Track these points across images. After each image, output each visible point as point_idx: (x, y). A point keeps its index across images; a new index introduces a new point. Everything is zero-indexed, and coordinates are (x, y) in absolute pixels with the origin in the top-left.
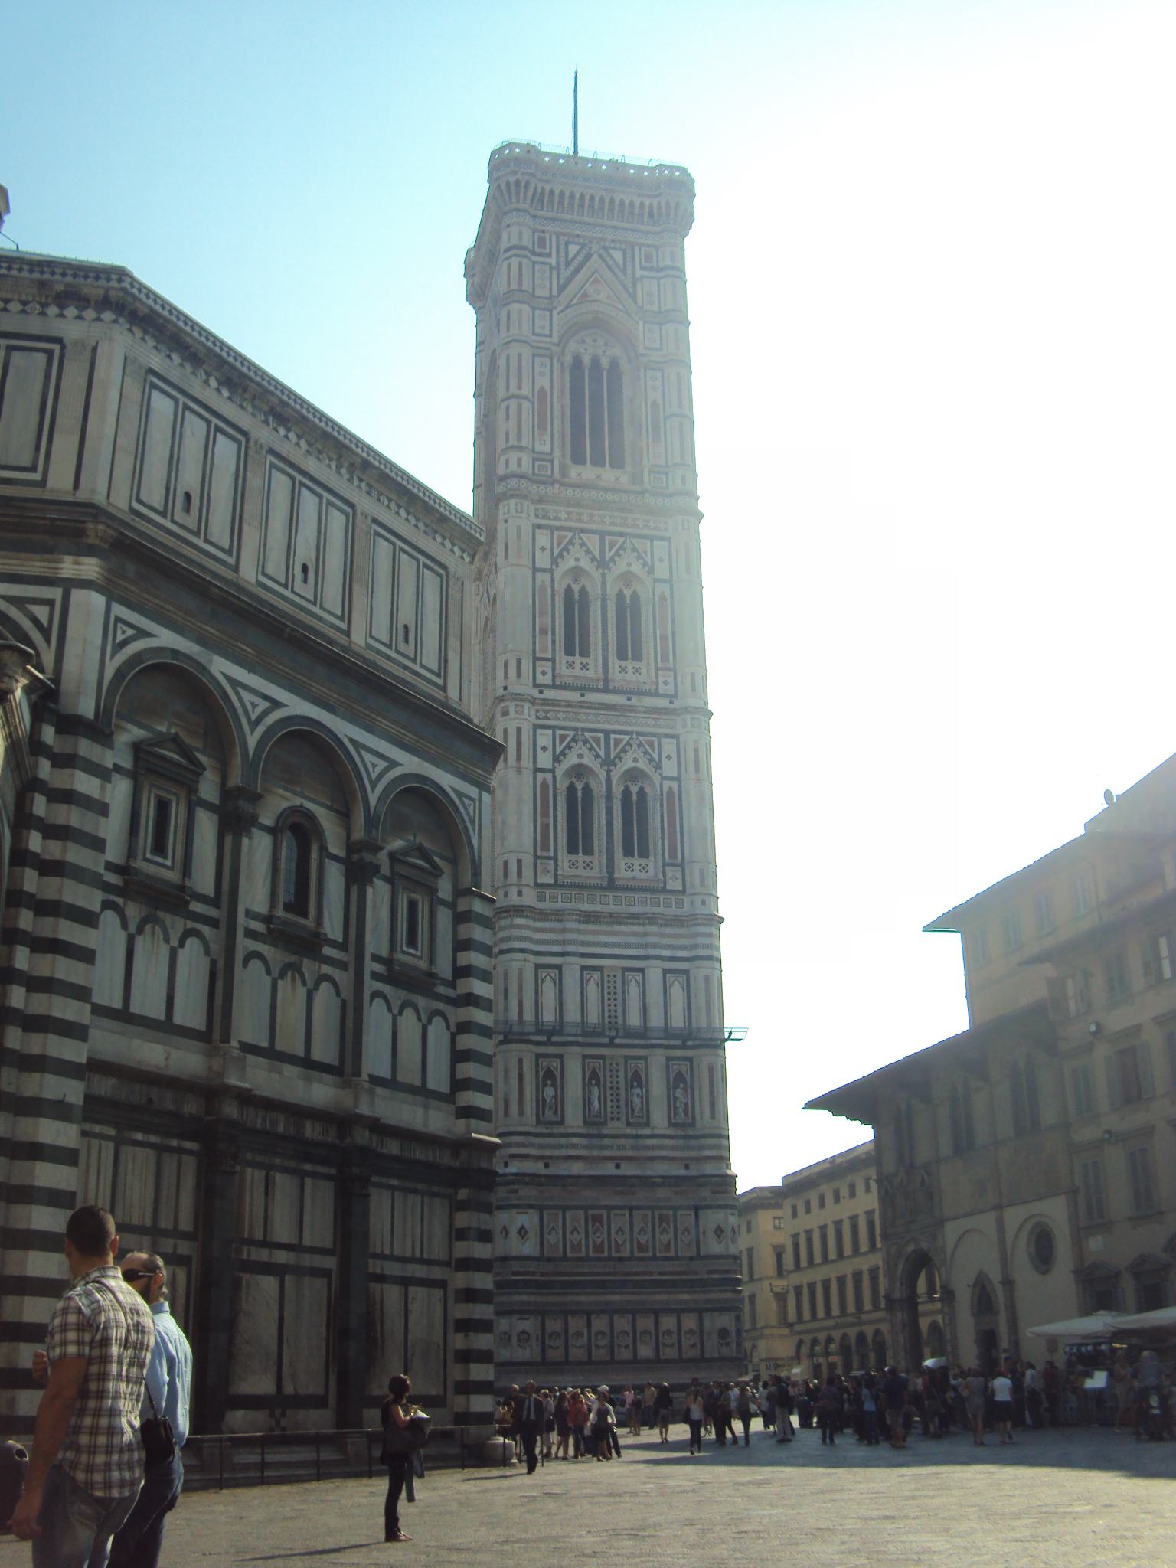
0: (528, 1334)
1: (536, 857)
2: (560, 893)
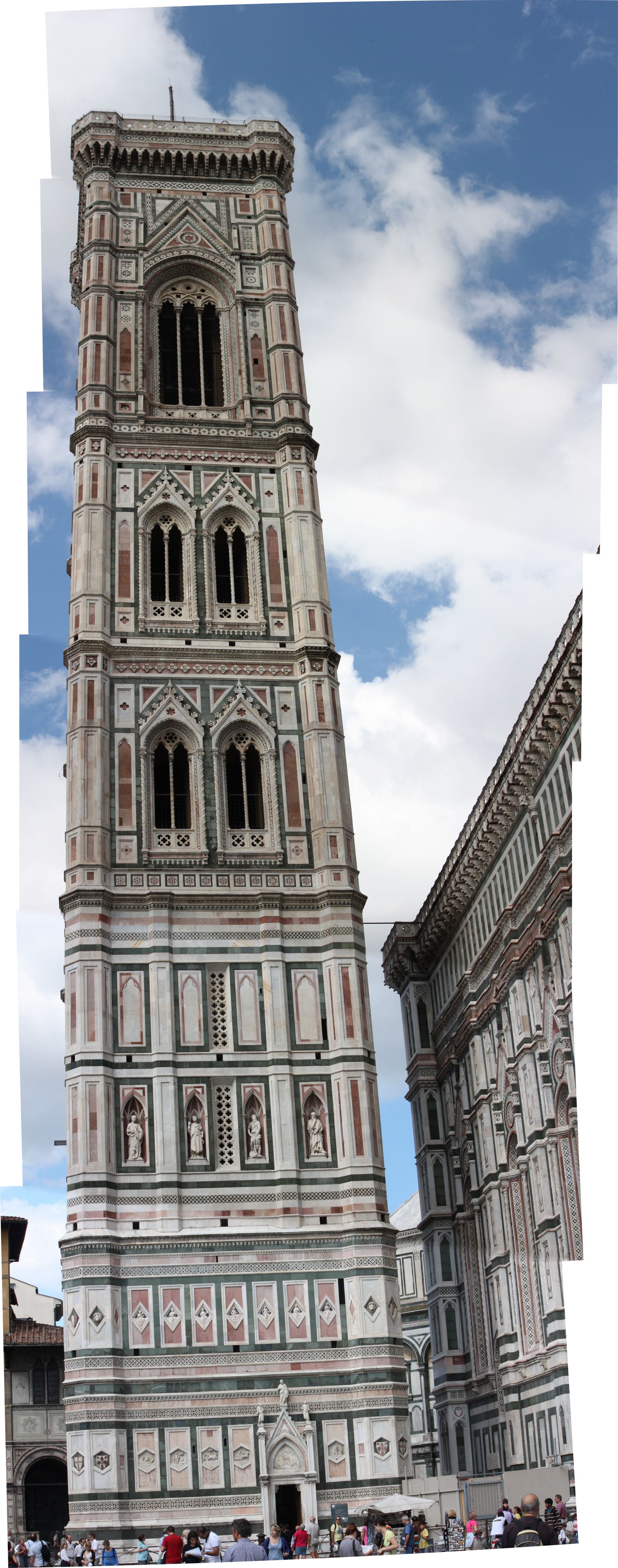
0: (108, 1456)
2: (145, 875)
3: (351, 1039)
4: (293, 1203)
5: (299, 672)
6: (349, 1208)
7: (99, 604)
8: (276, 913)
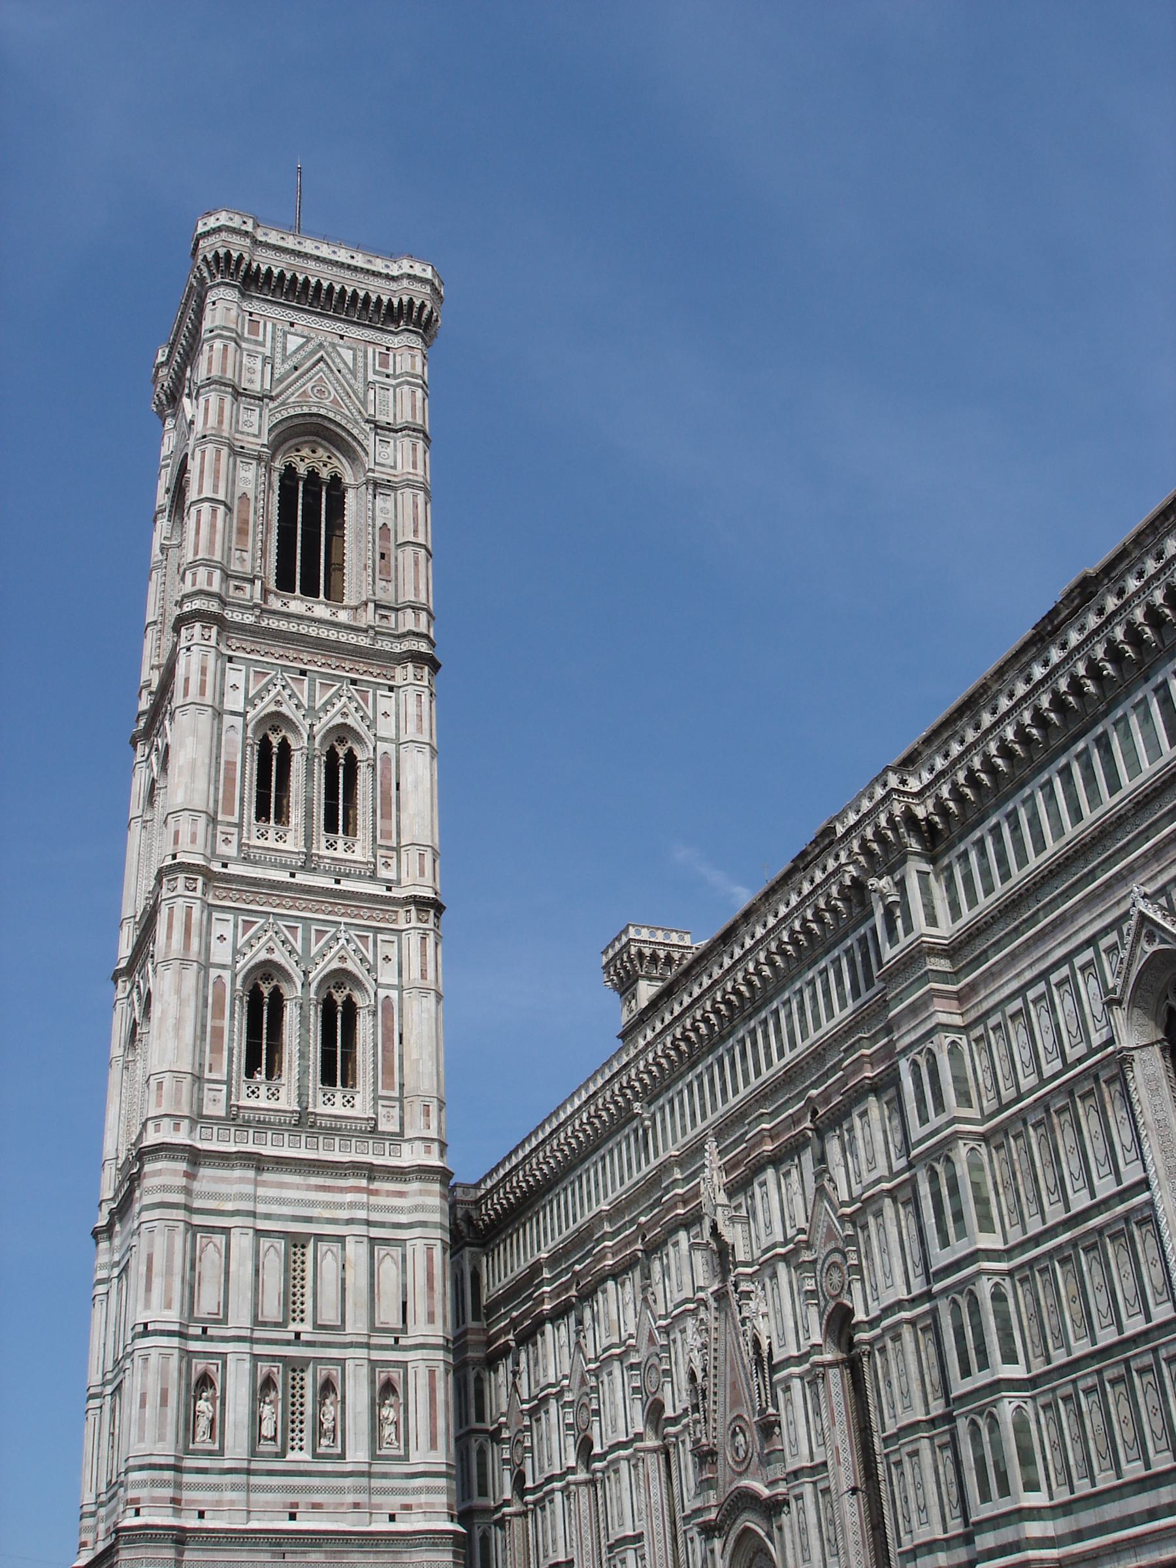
3: (432, 1326)
4: (362, 1498)
5: (404, 921)
6: (420, 1506)
7: (202, 820)
8: (364, 1183)
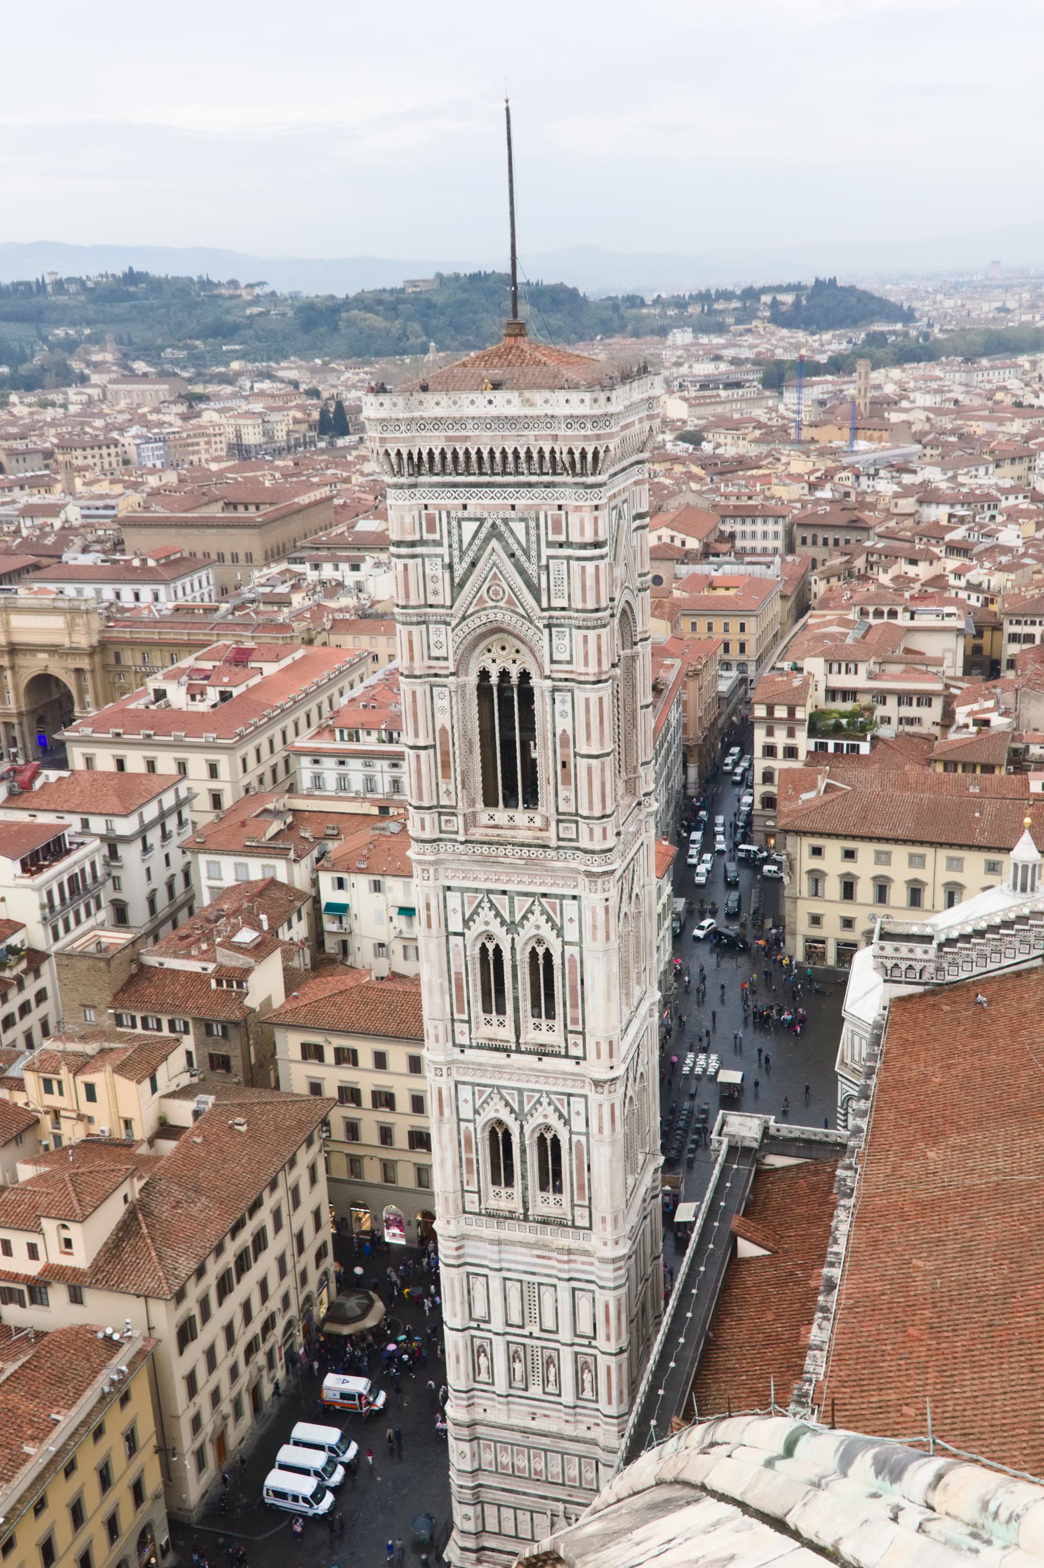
1: (463, 1191)
